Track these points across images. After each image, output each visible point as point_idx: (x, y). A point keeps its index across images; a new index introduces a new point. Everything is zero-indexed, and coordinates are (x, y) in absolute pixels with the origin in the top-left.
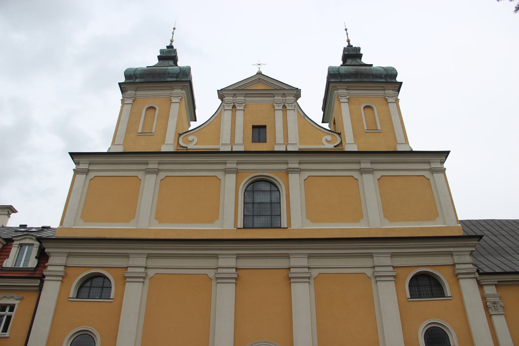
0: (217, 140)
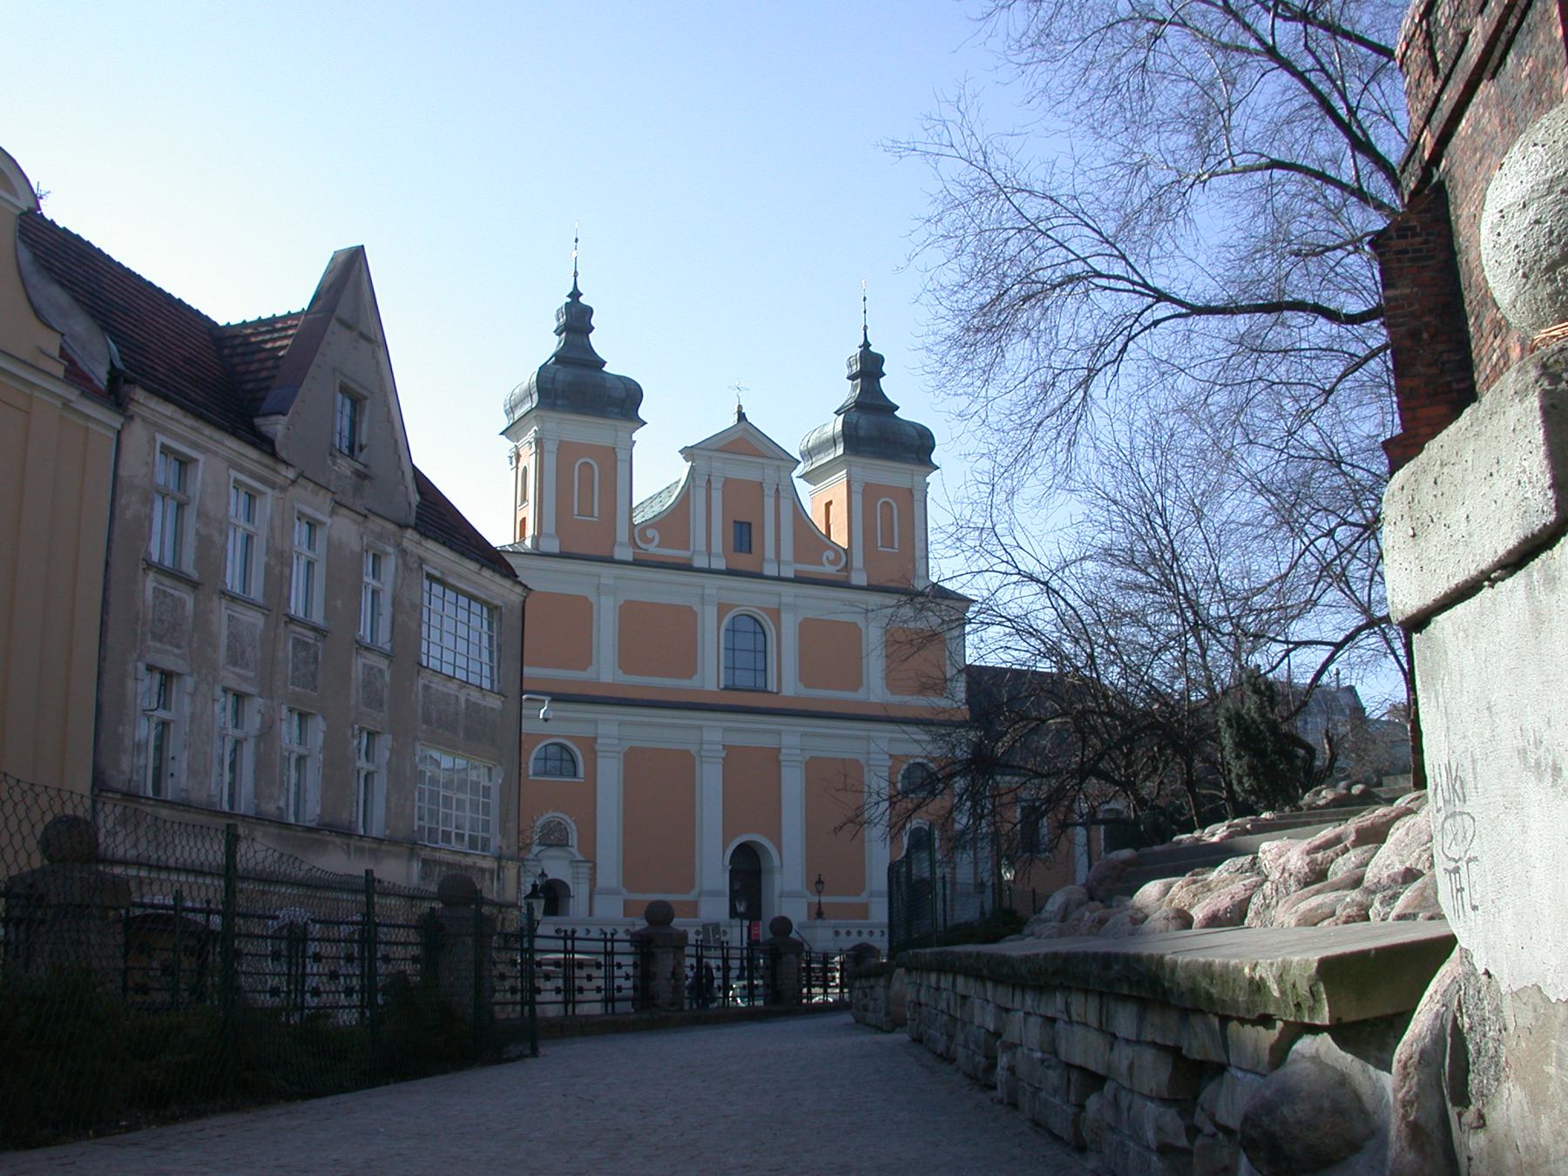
0: (685, 545)
